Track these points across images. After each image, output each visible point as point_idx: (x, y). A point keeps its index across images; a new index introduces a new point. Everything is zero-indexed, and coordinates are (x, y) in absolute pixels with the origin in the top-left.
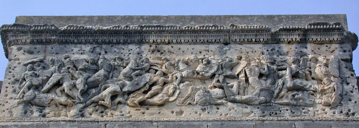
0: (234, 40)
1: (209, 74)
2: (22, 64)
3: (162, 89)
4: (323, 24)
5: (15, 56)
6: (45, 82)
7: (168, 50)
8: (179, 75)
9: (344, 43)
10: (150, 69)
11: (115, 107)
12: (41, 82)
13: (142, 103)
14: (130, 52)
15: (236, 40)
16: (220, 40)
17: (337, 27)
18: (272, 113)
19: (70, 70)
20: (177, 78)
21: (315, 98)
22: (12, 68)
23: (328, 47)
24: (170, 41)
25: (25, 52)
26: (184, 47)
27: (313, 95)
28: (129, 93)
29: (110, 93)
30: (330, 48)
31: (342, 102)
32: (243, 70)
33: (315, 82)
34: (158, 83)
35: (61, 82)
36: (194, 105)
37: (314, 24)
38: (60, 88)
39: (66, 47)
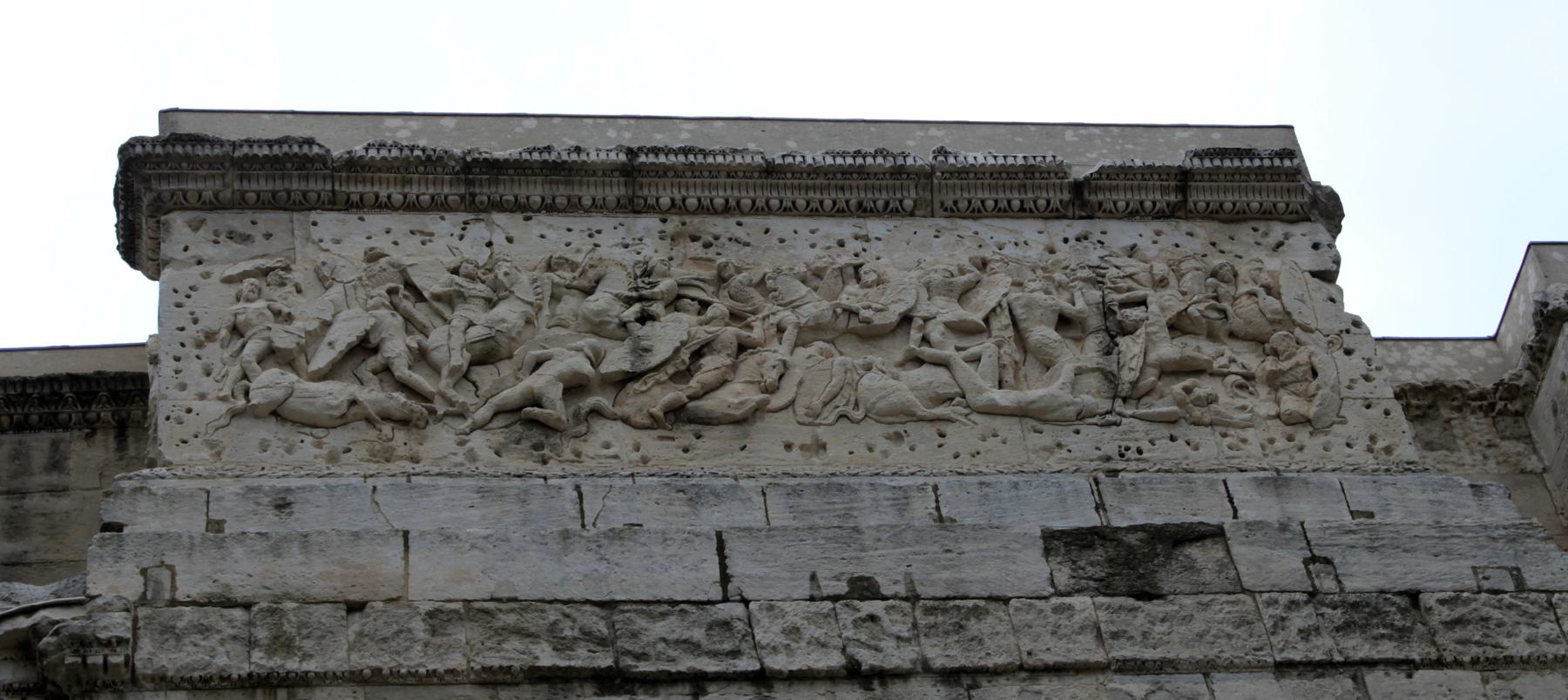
0: (949, 203)
1: (892, 316)
2: (216, 277)
3: (734, 368)
5: (186, 249)
8: (787, 316)
9: (1309, 220)
10: (680, 297)
11: (583, 428)
13: (677, 414)
15: (955, 203)
16: (901, 202)
17: (1287, 163)
18: (1127, 449)
19: (395, 299)
20: (781, 330)
22: (184, 290)
24: (732, 203)
25: (216, 233)
26: (782, 226)
27: (1241, 387)
28: (624, 380)
29: (560, 378)
30: (1266, 234)
31: (1342, 413)
32: (1005, 305)
34: (717, 345)
35: (374, 340)
36: (859, 422)
38: (374, 362)
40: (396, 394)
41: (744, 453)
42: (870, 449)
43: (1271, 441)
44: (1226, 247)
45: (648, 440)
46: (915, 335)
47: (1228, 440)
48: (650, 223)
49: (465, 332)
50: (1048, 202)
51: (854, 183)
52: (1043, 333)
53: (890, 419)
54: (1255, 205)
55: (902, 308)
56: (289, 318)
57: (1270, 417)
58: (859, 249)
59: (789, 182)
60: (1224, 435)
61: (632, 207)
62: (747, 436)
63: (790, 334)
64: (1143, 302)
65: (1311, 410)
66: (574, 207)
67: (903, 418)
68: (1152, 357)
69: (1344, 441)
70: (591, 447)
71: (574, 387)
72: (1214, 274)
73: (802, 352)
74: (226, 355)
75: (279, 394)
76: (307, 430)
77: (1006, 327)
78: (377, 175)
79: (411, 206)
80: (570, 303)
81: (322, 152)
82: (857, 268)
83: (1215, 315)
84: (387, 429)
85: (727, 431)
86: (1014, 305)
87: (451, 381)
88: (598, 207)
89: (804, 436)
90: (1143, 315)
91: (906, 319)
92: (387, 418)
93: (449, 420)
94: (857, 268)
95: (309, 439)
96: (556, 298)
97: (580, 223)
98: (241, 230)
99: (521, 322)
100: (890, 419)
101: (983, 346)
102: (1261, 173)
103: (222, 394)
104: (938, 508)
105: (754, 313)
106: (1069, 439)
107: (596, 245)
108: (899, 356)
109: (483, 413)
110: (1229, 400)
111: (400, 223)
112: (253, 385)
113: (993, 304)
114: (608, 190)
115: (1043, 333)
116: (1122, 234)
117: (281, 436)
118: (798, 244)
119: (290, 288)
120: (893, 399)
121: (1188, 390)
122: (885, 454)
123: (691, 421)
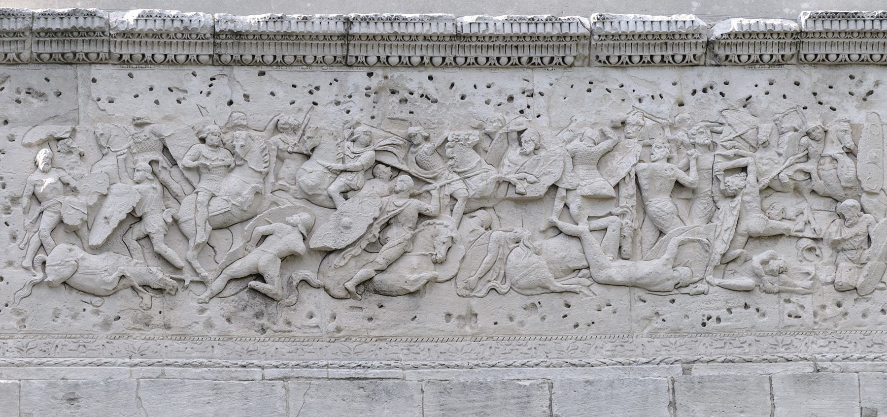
0: (603, 58)
1: (540, 189)
3: (413, 239)
4: (847, 17)
6: (94, 209)
7: (421, 92)
8: (458, 187)
11: (293, 298)
12: (85, 217)
14: (312, 98)
15: (608, 58)
16: (563, 58)
18: (709, 319)
19: (157, 169)
21: (817, 261)
23: (855, 80)
26: (465, 79)
27: (811, 249)
28: (328, 252)
32: (633, 175)
33: (818, 203)
34: (401, 219)
37: (823, 17)
38: (138, 230)
39: (130, 76)
40: (154, 269)
41: (414, 324)
42: (511, 319)
43: (824, 307)
44: (824, 98)
45: (341, 307)
46: (559, 205)
47: (790, 308)
48: (357, 78)
49: (209, 205)
50: (684, 56)
51: (526, 44)
52: (661, 203)
53: (529, 292)
54: (855, 57)
55: (549, 181)
56: (74, 191)
57: (827, 284)
58: (524, 107)
59: (473, 44)
60: (788, 301)
61: (346, 63)
62: (418, 307)
63: (459, 207)
64: (744, 169)
65: (860, 281)
66: (301, 62)
67: (540, 291)
68: (743, 227)
69: (880, 308)
70: (299, 318)
71: (289, 258)
72: (808, 134)
73: (471, 223)
74: (27, 222)
75: (66, 272)
76: (88, 298)
77: (632, 196)
78: (144, 40)
79: (170, 62)
80: (291, 166)
81: (102, 24)
82: (520, 133)
83: (801, 177)
84: (147, 296)
85: (402, 301)
86: (639, 176)
87: (195, 253)
88: (320, 62)
89: (460, 309)
90: (742, 184)
91: (554, 187)
92: (145, 286)
93: (194, 287)
94: (520, 133)
95: (89, 308)
96: (280, 159)
97: (305, 78)
98: (37, 88)
99: (251, 197)
100: (529, 292)
101: (612, 223)
102: (862, 33)
103: (25, 264)
104: (550, 406)
105: (435, 178)
106: (666, 309)
107: (315, 104)
108: (543, 226)
109: (217, 284)
110: (797, 265)
111: (160, 77)
112: (48, 260)
113: (623, 174)
114: (327, 49)
115: (661, 203)
116: (744, 82)
117: (70, 306)
118: (478, 97)
119: (74, 157)
120: (532, 277)
121: (765, 263)
122: (522, 323)
123: (376, 292)
